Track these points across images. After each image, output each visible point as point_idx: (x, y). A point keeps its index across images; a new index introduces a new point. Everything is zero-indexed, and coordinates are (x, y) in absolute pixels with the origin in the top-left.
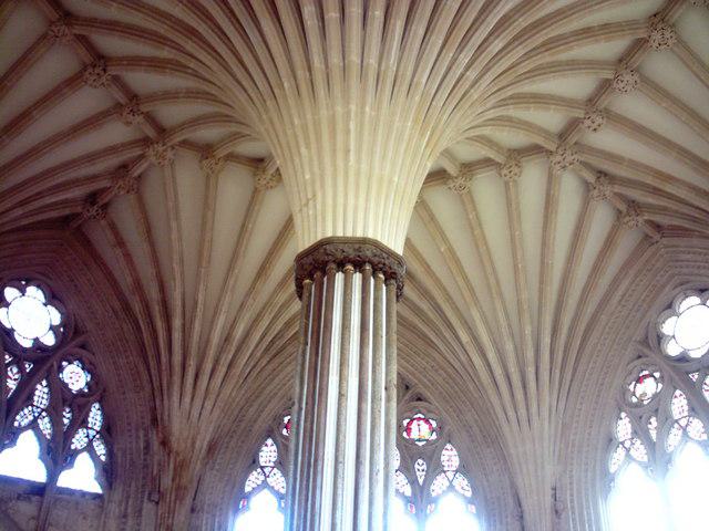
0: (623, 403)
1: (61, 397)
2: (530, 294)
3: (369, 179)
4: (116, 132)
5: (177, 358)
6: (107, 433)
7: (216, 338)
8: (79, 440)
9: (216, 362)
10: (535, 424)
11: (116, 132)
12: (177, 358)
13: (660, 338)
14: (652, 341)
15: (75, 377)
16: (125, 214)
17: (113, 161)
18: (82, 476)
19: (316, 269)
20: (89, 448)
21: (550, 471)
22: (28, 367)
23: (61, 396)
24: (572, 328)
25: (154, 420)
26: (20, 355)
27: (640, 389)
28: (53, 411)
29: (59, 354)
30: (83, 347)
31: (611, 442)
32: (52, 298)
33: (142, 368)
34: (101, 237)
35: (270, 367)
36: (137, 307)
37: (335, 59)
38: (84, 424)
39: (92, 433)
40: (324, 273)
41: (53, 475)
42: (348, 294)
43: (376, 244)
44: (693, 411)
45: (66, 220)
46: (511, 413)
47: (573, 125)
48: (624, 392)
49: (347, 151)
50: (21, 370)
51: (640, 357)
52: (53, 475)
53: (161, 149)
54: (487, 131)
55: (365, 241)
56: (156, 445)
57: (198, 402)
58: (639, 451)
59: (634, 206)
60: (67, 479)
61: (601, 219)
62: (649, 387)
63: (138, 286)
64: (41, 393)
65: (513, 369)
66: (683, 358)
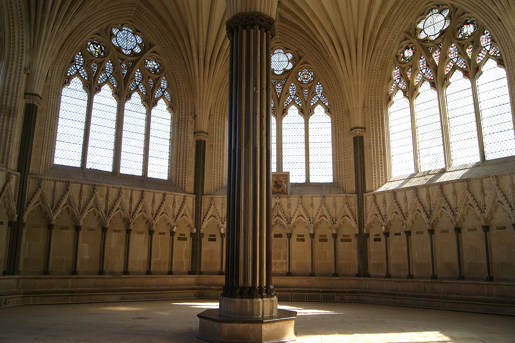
8: (158, 93)
15: (151, 64)
24: (374, 26)
30: (154, 52)
46: (344, 69)
51: (406, 39)
62: (408, 53)
64: (138, 74)
66: (426, 40)
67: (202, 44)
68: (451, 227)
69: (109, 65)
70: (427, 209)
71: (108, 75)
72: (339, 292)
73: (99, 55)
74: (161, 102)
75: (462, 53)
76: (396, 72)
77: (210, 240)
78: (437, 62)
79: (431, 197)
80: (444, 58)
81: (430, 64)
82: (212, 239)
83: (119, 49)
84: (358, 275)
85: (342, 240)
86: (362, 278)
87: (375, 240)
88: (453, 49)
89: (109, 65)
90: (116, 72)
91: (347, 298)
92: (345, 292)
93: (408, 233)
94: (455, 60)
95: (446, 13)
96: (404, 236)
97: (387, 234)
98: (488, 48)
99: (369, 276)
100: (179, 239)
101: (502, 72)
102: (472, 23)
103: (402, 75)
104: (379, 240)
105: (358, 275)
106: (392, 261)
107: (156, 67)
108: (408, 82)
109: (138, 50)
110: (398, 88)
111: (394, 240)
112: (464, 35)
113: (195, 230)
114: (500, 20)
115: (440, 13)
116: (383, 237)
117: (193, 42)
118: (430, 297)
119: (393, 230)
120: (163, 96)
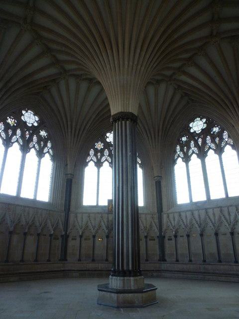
1: (40, 139)
4: (52, 71)
8: (46, 150)
15: (43, 133)
22: (31, 132)
26: (28, 128)
28: (38, 143)
30: (45, 126)
31: (175, 152)
44: (195, 146)
47: (174, 74)
50: (29, 132)
59: (186, 94)
61: (178, 97)
62: (184, 139)
64: (35, 138)
67: (74, 124)
68: (213, 232)
69: (19, 132)
70: (199, 223)
71: (18, 137)
72: (150, 271)
73: (13, 125)
74: (47, 155)
75: (213, 141)
76: (178, 147)
77: (73, 239)
78: (200, 145)
79: (201, 216)
80: (204, 143)
81: (196, 145)
82: (74, 239)
83: (25, 122)
84: (159, 260)
85: (150, 240)
86: (162, 262)
87: (169, 240)
88: (208, 138)
89: (19, 132)
90: (23, 136)
91: (155, 274)
92: (153, 271)
93: (188, 236)
94: (209, 144)
95: (204, 120)
96: (185, 237)
97: (176, 236)
98: (226, 140)
99: (166, 261)
100: (55, 239)
101: (234, 152)
102: (218, 127)
103: (182, 150)
104: (171, 239)
105: (159, 260)
106: (179, 252)
107: (45, 135)
108: (184, 153)
109: (36, 124)
110: (179, 156)
111: (180, 239)
112: (214, 132)
113: (63, 233)
114: (234, 126)
115: (201, 120)
116: (173, 238)
117: (69, 123)
118: (204, 273)
119: (179, 234)
120: (48, 152)
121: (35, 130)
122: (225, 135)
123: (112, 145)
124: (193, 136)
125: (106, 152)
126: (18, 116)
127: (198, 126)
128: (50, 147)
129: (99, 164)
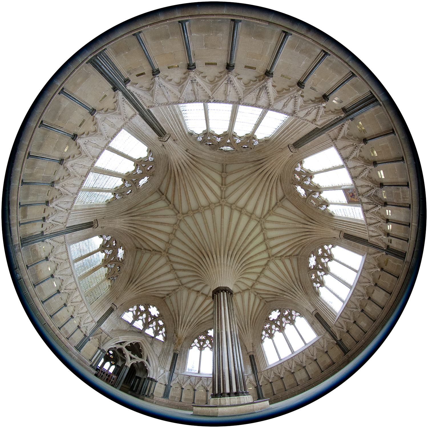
0: (263, 329)
1: (158, 325)
2: (246, 314)
3: (226, 280)
5: (180, 323)
6: (166, 332)
7: (188, 321)
8: (160, 332)
9: (187, 325)
10: (248, 334)
11: (174, 283)
12: (180, 323)
13: (269, 318)
14: (267, 319)
15: (161, 323)
16: (173, 298)
17: (173, 288)
18: (160, 338)
19: (217, 292)
20: (162, 334)
21: (251, 341)
23: (158, 325)
25: (175, 332)
26: (151, 316)
27: (266, 327)
28: (156, 326)
29: (159, 318)
31: (262, 335)
32: (158, 310)
33: (173, 324)
34: (168, 302)
35: (197, 328)
36: (173, 314)
37: (219, 262)
38: (162, 330)
39: (163, 332)
40: (219, 292)
41: (155, 336)
42: (223, 296)
43: (228, 288)
45: (162, 298)
48: (263, 327)
49: (222, 275)
50: (151, 318)
52: (155, 336)
53: (182, 287)
54: (242, 276)
55: (226, 287)
56: (175, 336)
57: (184, 330)
58: (267, 335)
60: (157, 337)
62: (268, 326)
63: (174, 311)
65: (243, 326)
81: (277, 326)
88: (284, 319)
90: (147, 319)
95: (278, 311)
108: (269, 334)
121: (155, 318)
122: (293, 313)
123: (212, 338)
124: (273, 322)
125: (208, 342)
126: (147, 306)
127: (274, 315)
128: (164, 331)
129: (201, 348)
